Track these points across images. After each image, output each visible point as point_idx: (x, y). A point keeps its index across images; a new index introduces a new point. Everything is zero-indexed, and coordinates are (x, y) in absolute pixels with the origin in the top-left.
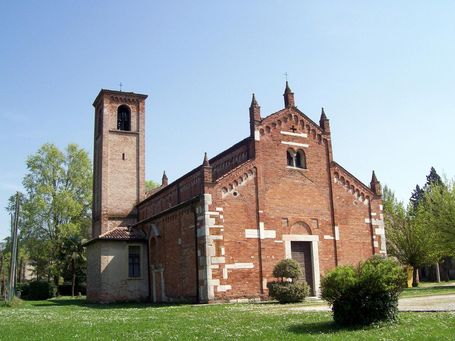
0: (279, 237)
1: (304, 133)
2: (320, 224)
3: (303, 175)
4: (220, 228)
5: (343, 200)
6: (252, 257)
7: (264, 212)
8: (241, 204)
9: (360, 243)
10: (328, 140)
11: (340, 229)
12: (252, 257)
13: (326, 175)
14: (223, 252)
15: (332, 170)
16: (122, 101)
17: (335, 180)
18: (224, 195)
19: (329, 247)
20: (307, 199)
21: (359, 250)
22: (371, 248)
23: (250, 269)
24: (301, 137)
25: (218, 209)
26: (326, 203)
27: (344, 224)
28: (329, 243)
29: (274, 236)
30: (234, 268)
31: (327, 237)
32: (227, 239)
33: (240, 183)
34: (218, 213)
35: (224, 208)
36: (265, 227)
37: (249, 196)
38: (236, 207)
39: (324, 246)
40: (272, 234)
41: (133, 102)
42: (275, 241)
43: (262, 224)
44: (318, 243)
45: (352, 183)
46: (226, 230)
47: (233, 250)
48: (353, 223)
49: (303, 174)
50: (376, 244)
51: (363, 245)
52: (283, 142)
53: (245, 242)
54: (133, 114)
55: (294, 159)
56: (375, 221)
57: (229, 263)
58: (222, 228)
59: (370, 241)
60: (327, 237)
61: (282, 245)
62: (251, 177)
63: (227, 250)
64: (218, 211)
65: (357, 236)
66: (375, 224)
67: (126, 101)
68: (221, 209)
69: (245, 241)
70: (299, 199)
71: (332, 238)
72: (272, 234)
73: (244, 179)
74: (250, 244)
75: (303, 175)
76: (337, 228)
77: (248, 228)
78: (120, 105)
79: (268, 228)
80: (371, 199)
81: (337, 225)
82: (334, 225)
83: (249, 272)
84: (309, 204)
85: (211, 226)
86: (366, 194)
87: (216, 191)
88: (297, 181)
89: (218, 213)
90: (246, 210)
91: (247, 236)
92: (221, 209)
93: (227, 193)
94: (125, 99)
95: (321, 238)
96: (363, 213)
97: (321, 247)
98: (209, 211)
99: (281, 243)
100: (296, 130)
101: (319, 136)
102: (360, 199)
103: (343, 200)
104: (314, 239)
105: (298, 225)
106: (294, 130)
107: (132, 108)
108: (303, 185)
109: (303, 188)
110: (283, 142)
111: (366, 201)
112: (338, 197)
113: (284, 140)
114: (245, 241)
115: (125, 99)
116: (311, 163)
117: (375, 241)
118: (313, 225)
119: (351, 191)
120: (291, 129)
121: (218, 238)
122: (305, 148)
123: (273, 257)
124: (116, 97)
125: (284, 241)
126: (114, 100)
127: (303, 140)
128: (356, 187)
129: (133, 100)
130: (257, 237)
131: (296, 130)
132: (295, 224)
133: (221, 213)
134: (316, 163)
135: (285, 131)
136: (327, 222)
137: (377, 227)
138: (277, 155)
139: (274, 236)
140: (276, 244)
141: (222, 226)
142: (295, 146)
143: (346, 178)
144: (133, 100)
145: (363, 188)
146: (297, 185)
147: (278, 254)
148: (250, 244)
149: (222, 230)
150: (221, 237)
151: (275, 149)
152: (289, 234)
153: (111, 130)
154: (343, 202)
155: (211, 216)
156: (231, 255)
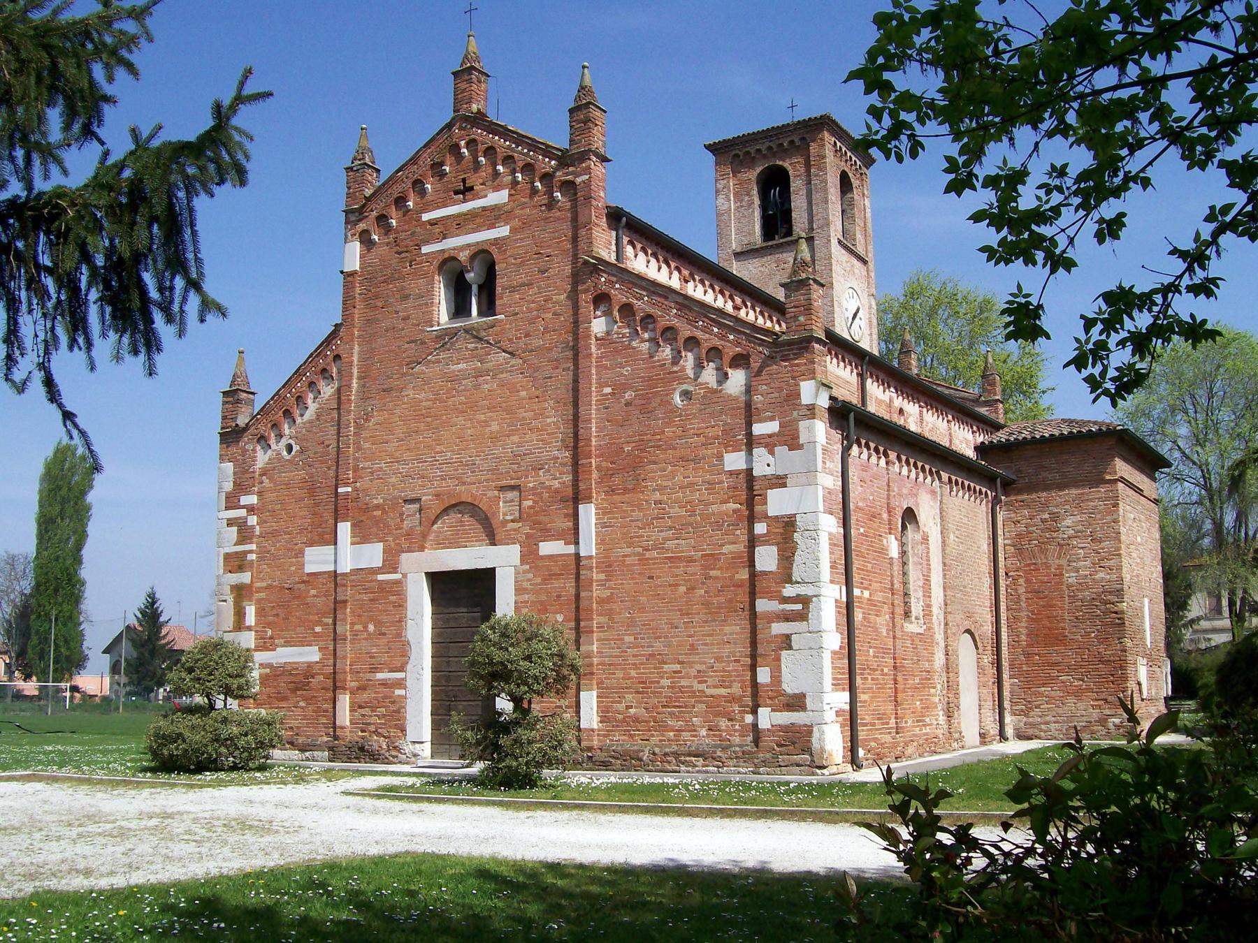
0: (391, 564)
1: (497, 189)
2: (530, 503)
3: (481, 339)
4: (246, 553)
5: (629, 395)
6: (318, 629)
7: (355, 489)
9: (691, 560)
10: (579, 180)
11: (602, 512)
12: (318, 629)
13: (566, 317)
15: (586, 291)
16: (764, 157)
17: (598, 326)
18: (262, 458)
19: (557, 584)
20: (486, 423)
21: (683, 589)
22: (744, 575)
23: (310, 665)
24: (484, 209)
25: (244, 500)
26: (555, 419)
27: (626, 491)
29: (378, 562)
30: (274, 661)
31: (549, 548)
32: (263, 580)
33: (302, 415)
34: (243, 512)
35: (260, 494)
36: (354, 535)
37: (320, 449)
38: (288, 485)
39: (539, 580)
41: (784, 152)
42: (381, 577)
43: (345, 529)
44: (517, 573)
45: (671, 318)
46: (262, 553)
47: (274, 612)
48: (666, 484)
49: (483, 334)
50: (767, 559)
51: (705, 567)
52: (425, 249)
53: (302, 586)
54: (796, 184)
55: (475, 289)
56: (770, 459)
58: (251, 552)
59: (741, 547)
60: (549, 548)
61: (396, 591)
62: (327, 390)
63: (260, 613)
64: (243, 507)
65: (680, 529)
66: (769, 471)
67: (774, 155)
68: (252, 499)
69: (303, 582)
70: (464, 428)
71: (571, 549)
72: (373, 555)
73: (310, 401)
74: (313, 592)
75: (481, 339)
76: (589, 514)
77: (311, 544)
78: (759, 169)
79: (361, 536)
80: (755, 365)
81: (588, 499)
82: (577, 497)
83: (309, 671)
84: (494, 438)
85: (228, 550)
86: (731, 351)
87: (245, 451)
88: (462, 366)
90: (312, 491)
91: (309, 569)
92: (252, 499)
93: (269, 452)
94: (770, 148)
95: (530, 555)
96: (711, 432)
97: (526, 585)
98: (227, 508)
99: (398, 582)
100: (471, 189)
101: (547, 177)
102: (709, 375)
103: (629, 395)
104: (504, 560)
105: (453, 517)
106: (466, 191)
107: (794, 166)
108: (479, 374)
109: (477, 387)
110: (425, 249)
111: (737, 379)
113: (427, 242)
114: (303, 582)
115: (770, 148)
116: (513, 289)
117: (767, 543)
118: (505, 509)
119: (666, 352)
120: (456, 193)
121: (239, 581)
122: (496, 242)
123: (371, 628)
124: (759, 151)
125: (405, 576)
126: (741, 164)
127: (491, 216)
128: (686, 331)
130: (332, 568)
131: (471, 189)
132: (446, 511)
133: (251, 509)
134: (530, 285)
135: (439, 208)
136: (557, 491)
137: (779, 481)
138: (405, 297)
139: (378, 562)
141: (254, 547)
142: (462, 248)
143: (642, 304)
144: (792, 142)
145: (721, 325)
146: (454, 379)
147: (385, 619)
148: (313, 592)
149: (254, 557)
150: (246, 578)
151: (402, 278)
152: (422, 549)
153: (738, 250)
154: (628, 404)
155: (230, 523)
156: (269, 625)
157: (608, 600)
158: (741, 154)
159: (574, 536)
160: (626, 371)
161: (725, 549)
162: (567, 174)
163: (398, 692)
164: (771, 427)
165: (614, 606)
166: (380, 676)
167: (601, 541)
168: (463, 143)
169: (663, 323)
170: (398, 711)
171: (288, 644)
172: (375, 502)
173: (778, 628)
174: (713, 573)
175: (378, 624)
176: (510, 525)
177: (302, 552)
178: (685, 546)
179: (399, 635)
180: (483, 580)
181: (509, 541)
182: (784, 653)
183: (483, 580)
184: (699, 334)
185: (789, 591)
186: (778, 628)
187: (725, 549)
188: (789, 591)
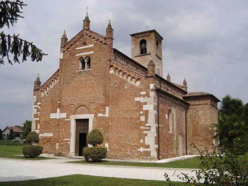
0: (68, 117)
2: (96, 106)
4: (38, 114)
5: (116, 86)
6: (53, 130)
8: (49, 99)
9: (128, 118)
10: (108, 43)
12: (53, 130)
14: (39, 128)
21: (126, 124)
23: (51, 137)
27: (115, 104)
28: (101, 119)
29: (65, 117)
31: (99, 115)
34: (38, 106)
35: (41, 102)
36: (60, 111)
39: (97, 121)
40: (64, 115)
42: (66, 120)
43: (58, 110)
44: (93, 120)
47: (44, 126)
50: (143, 118)
53: (50, 121)
55: (86, 64)
56: (144, 99)
57: (42, 133)
60: (99, 115)
61: (69, 122)
63: (41, 126)
66: (144, 101)
72: (64, 115)
74: (52, 122)
76: (107, 108)
77: (52, 113)
79: (62, 111)
83: (51, 138)
84: (90, 93)
88: (83, 79)
89: (38, 106)
91: (51, 118)
94: (143, 36)
95: (96, 116)
96: (132, 93)
97: (95, 122)
99: (69, 121)
100: (86, 44)
103: (116, 86)
104: (91, 117)
106: (85, 44)
110: (76, 55)
112: (112, 84)
113: (77, 54)
115: (143, 36)
116: (94, 64)
117: (143, 115)
120: (83, 44)
123: (63, 130)
127: (90, 49)
129: (147, 35)
131: (86, 44)
135: (80, 47)
136: (102, 104)
137: (146, 104)
138: (72, 65)
139: (65, 117)
140: (66, 122)
142: (84, 55)
144: (147, 35)
146: (82, 81)
148: (52, 122)
150: (38, 119)
152: (75, 114)
154: (116, 87)
155: (35, 108)
156: (43, 129)
157: (111, 125)
158: (137, 37)
159: (104, 113)
160: (116, 81)
161: (135, 116)
162: (105, 42)
163: (68, 143)
164: (144, 93)
165: (112, 126)
166: (65, 139)
167: (110, 114)
168: (85, 34)
169: (124, 72)
170: (69, 147)
171: (46, 132)
172: (65, 105)
173: (145, 132)
174: (132, 121)
175: (65, 129)
176: (92, 110)
177: (50, 114)
178: (127, 115)
179: (69, 131)
180: (87, 121)
181: (92, 113)
182: (146, 137)
183: (87, 121)
184: (131, 74)
185: (147, 125)
186: (145, 132)
187: (135, 116)
188: (147, 125)
